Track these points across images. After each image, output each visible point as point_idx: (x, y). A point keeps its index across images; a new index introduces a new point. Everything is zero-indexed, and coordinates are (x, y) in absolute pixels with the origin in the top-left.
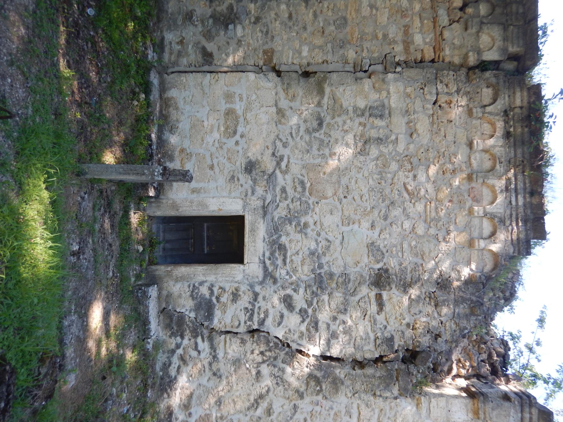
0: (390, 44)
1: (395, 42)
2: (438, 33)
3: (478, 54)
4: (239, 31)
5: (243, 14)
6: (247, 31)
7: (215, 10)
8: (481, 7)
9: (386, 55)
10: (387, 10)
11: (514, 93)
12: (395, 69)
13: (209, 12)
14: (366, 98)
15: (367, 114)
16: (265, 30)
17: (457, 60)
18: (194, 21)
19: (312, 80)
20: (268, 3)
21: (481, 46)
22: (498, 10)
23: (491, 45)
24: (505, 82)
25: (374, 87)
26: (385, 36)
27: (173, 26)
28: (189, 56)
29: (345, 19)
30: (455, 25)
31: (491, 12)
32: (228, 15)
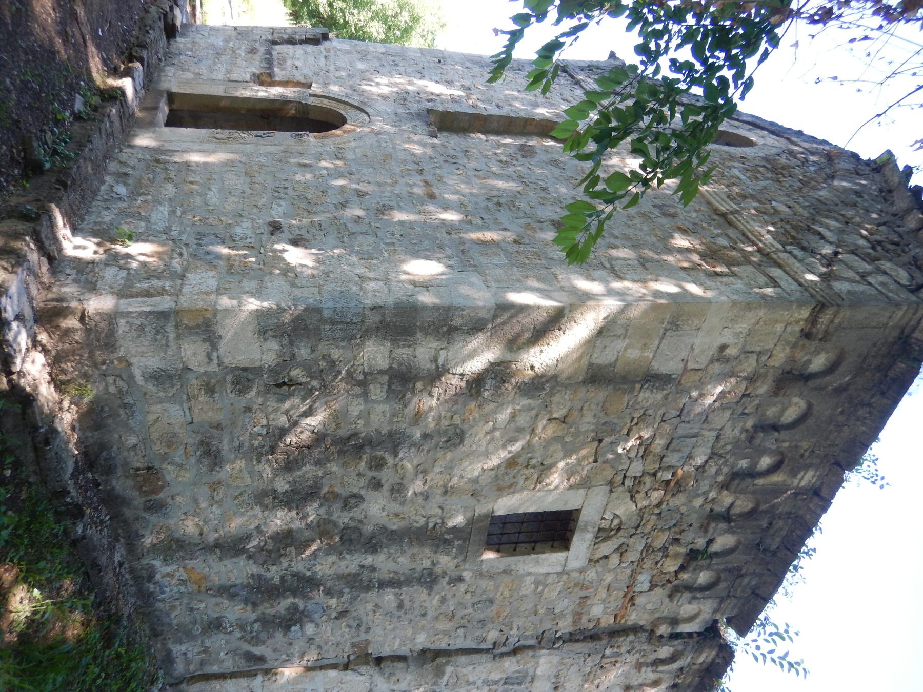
0: (554, 619)
1: (562, 615)
2: (629, 596)
3: (673, 628)
4: (310, 629)
5: (316, 612)
6: (324, 627)
7: (263, 613)
8: (701, 574)
9: (543, 632)
10: (561, 583)
11: (701, 653)
12: (554, 644)
13: (253, 617)
14: (504, 671)
15: (503, 681)
16: (355, 625)
17: (641, 623)
18: (225, 628)
19: (428, 666)
20: (363, 595)
21: (682, 612)
22: (723, 585)
23: (695, 612)
24: (693, 647)
25: (518, 662)
26: (550, 611)
27: (186, 634)
28: (223, 661)
29: (491, 602)
30: (658, 591)
31: (712, 580)
32: (288, 617)
